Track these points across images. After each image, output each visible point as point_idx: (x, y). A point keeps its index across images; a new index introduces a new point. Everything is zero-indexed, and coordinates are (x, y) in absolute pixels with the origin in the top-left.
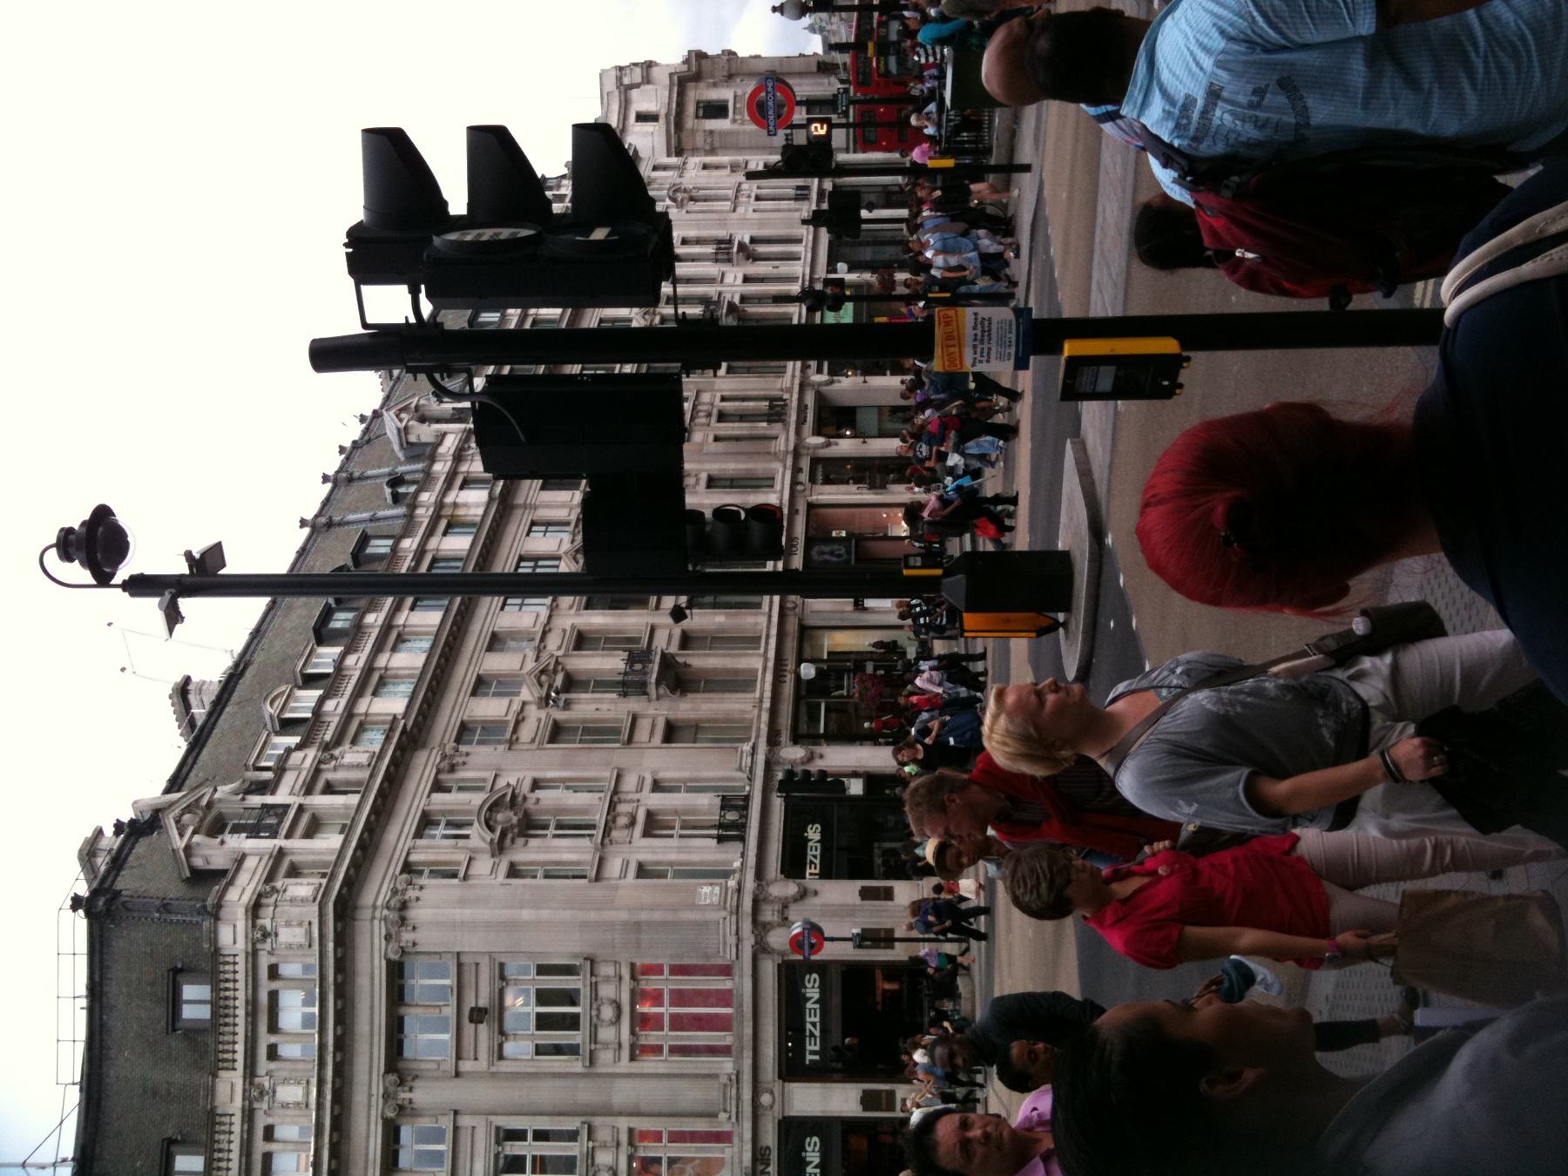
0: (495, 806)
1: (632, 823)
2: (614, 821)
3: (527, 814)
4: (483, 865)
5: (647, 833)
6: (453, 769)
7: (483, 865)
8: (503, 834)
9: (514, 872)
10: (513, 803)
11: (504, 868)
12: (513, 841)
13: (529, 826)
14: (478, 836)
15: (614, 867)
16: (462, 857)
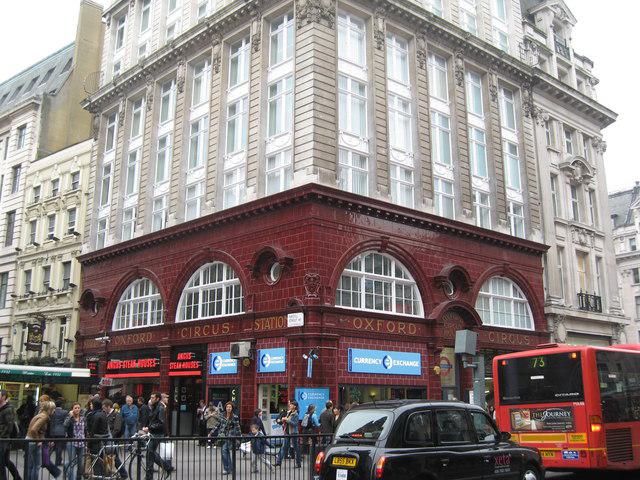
0: (584, 167)
1: (582, 244)
2: (584, 234)
3: (579, 185)
4: (555, 159)
5: (578, 251)
6: (595, 146)
7: (555, 159)
8: (571, 170)
9: (554, 177)
10: (585, 177)
11: (555, 171)
12: (568, 176)
13: (575, 187)
14: (567, 157)
15: (561, 231)
16: (557, 147)
